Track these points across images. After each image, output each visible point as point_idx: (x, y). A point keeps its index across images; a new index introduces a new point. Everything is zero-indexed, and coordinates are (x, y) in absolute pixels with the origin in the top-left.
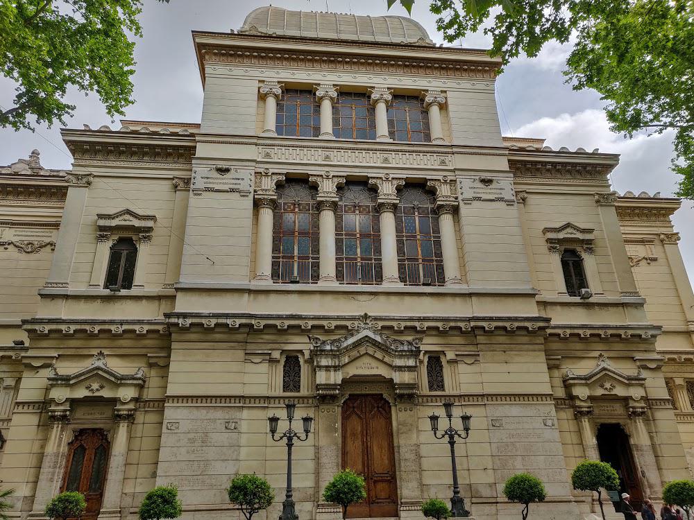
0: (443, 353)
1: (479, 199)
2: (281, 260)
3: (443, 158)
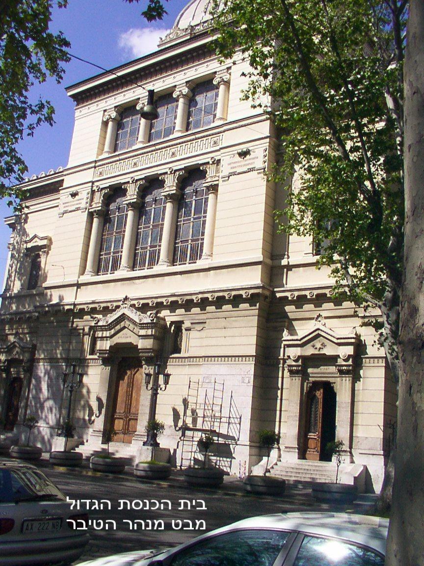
0: (182, 322)
1: (234, 174)
2: (104, 256)
3: (215, 139)
